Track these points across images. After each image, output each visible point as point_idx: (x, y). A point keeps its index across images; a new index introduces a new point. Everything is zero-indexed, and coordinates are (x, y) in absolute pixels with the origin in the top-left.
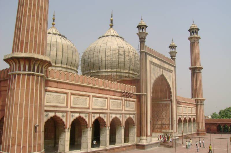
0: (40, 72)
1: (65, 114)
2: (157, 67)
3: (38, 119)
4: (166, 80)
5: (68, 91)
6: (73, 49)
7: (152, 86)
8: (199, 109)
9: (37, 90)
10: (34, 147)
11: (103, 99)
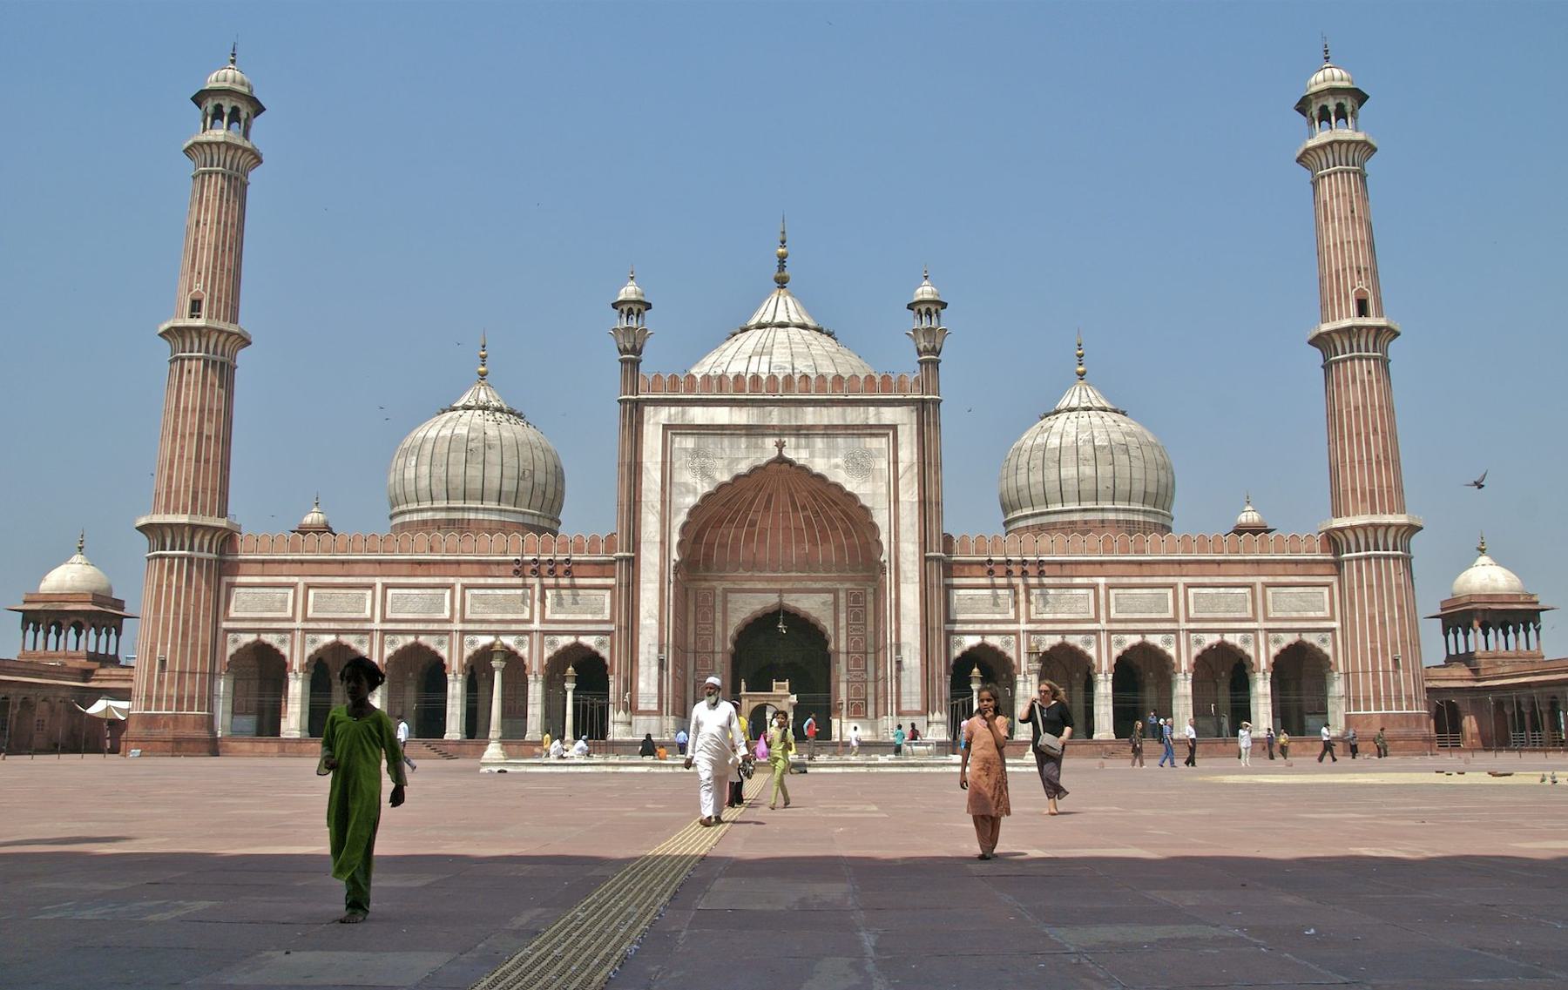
0: (177, 548)
1: (289, 636)
2: (726, 441)
3: (169, 646)
4: (821, 478)
5: (296, 579)
6: (472, 445)
7: (680, 519)
8: (1351, 589)
9: (169, 586)
10: (159, 699)
11: (429, 591)
